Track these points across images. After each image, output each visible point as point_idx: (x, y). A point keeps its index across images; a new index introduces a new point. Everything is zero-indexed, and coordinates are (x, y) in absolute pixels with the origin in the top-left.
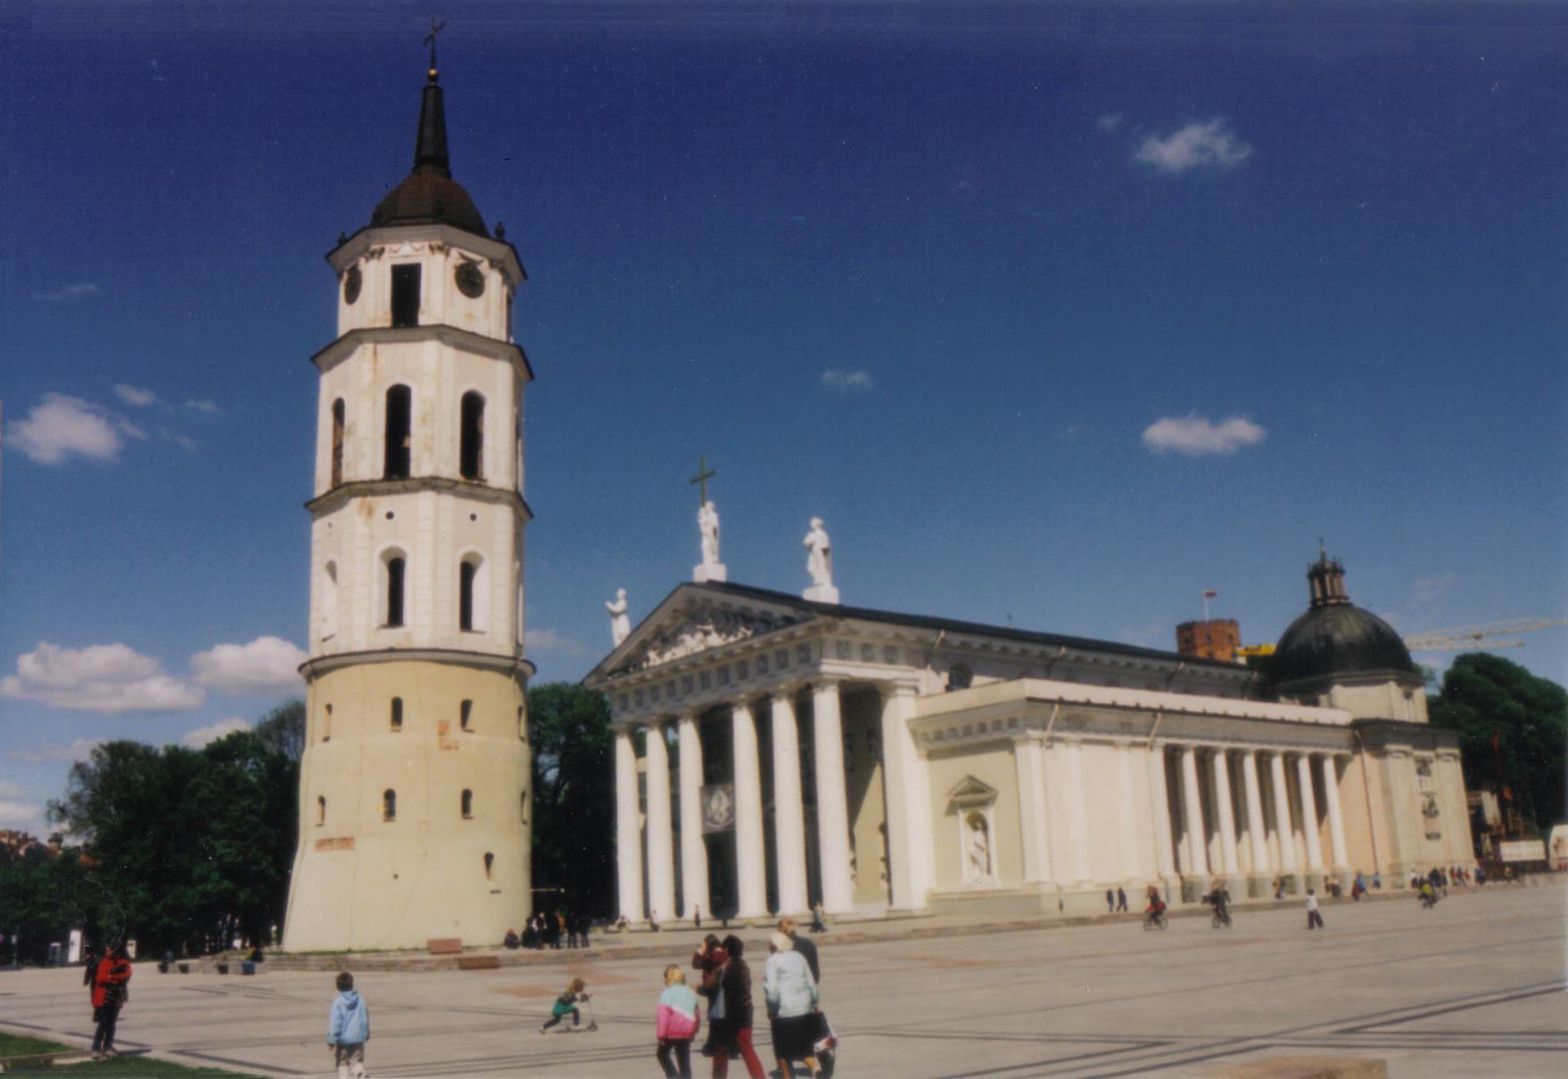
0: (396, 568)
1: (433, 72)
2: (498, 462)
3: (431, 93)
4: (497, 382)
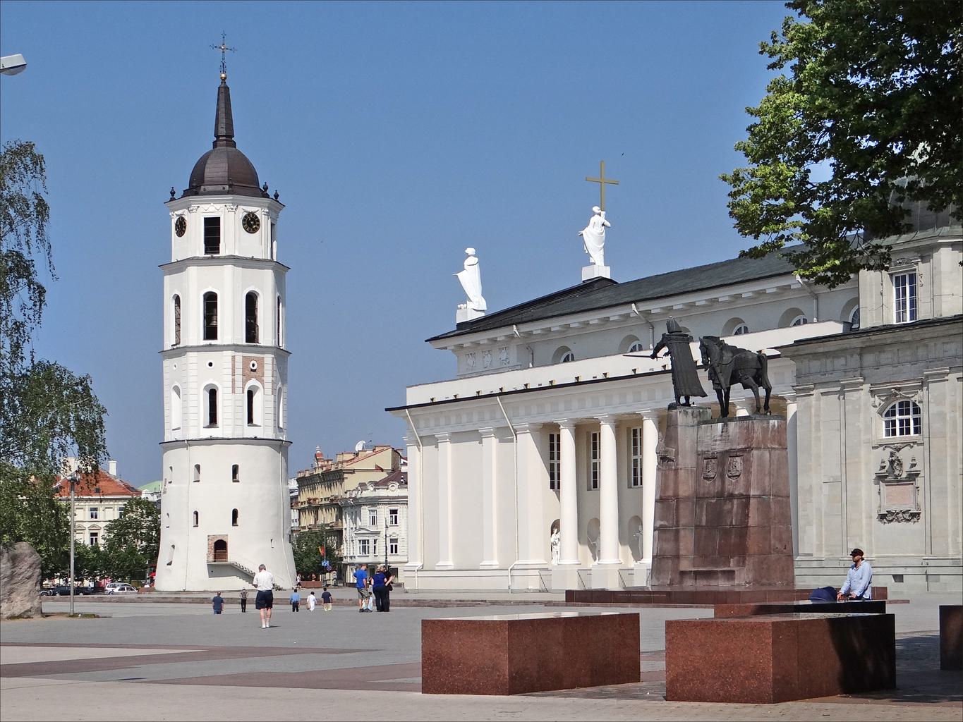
0: (213, 394)
1: (223, 75)
2: (266, 336)
3: (223, 90)
4: (264, 284)
